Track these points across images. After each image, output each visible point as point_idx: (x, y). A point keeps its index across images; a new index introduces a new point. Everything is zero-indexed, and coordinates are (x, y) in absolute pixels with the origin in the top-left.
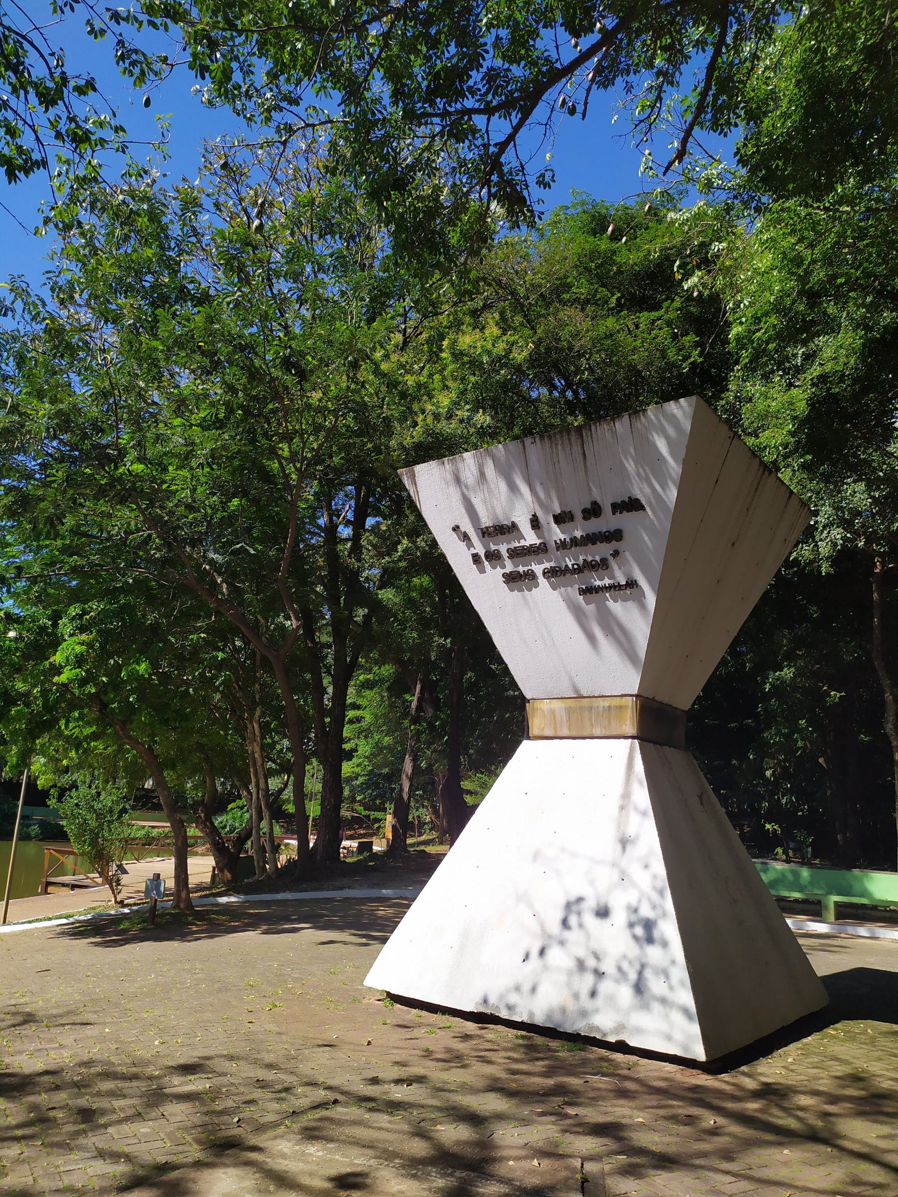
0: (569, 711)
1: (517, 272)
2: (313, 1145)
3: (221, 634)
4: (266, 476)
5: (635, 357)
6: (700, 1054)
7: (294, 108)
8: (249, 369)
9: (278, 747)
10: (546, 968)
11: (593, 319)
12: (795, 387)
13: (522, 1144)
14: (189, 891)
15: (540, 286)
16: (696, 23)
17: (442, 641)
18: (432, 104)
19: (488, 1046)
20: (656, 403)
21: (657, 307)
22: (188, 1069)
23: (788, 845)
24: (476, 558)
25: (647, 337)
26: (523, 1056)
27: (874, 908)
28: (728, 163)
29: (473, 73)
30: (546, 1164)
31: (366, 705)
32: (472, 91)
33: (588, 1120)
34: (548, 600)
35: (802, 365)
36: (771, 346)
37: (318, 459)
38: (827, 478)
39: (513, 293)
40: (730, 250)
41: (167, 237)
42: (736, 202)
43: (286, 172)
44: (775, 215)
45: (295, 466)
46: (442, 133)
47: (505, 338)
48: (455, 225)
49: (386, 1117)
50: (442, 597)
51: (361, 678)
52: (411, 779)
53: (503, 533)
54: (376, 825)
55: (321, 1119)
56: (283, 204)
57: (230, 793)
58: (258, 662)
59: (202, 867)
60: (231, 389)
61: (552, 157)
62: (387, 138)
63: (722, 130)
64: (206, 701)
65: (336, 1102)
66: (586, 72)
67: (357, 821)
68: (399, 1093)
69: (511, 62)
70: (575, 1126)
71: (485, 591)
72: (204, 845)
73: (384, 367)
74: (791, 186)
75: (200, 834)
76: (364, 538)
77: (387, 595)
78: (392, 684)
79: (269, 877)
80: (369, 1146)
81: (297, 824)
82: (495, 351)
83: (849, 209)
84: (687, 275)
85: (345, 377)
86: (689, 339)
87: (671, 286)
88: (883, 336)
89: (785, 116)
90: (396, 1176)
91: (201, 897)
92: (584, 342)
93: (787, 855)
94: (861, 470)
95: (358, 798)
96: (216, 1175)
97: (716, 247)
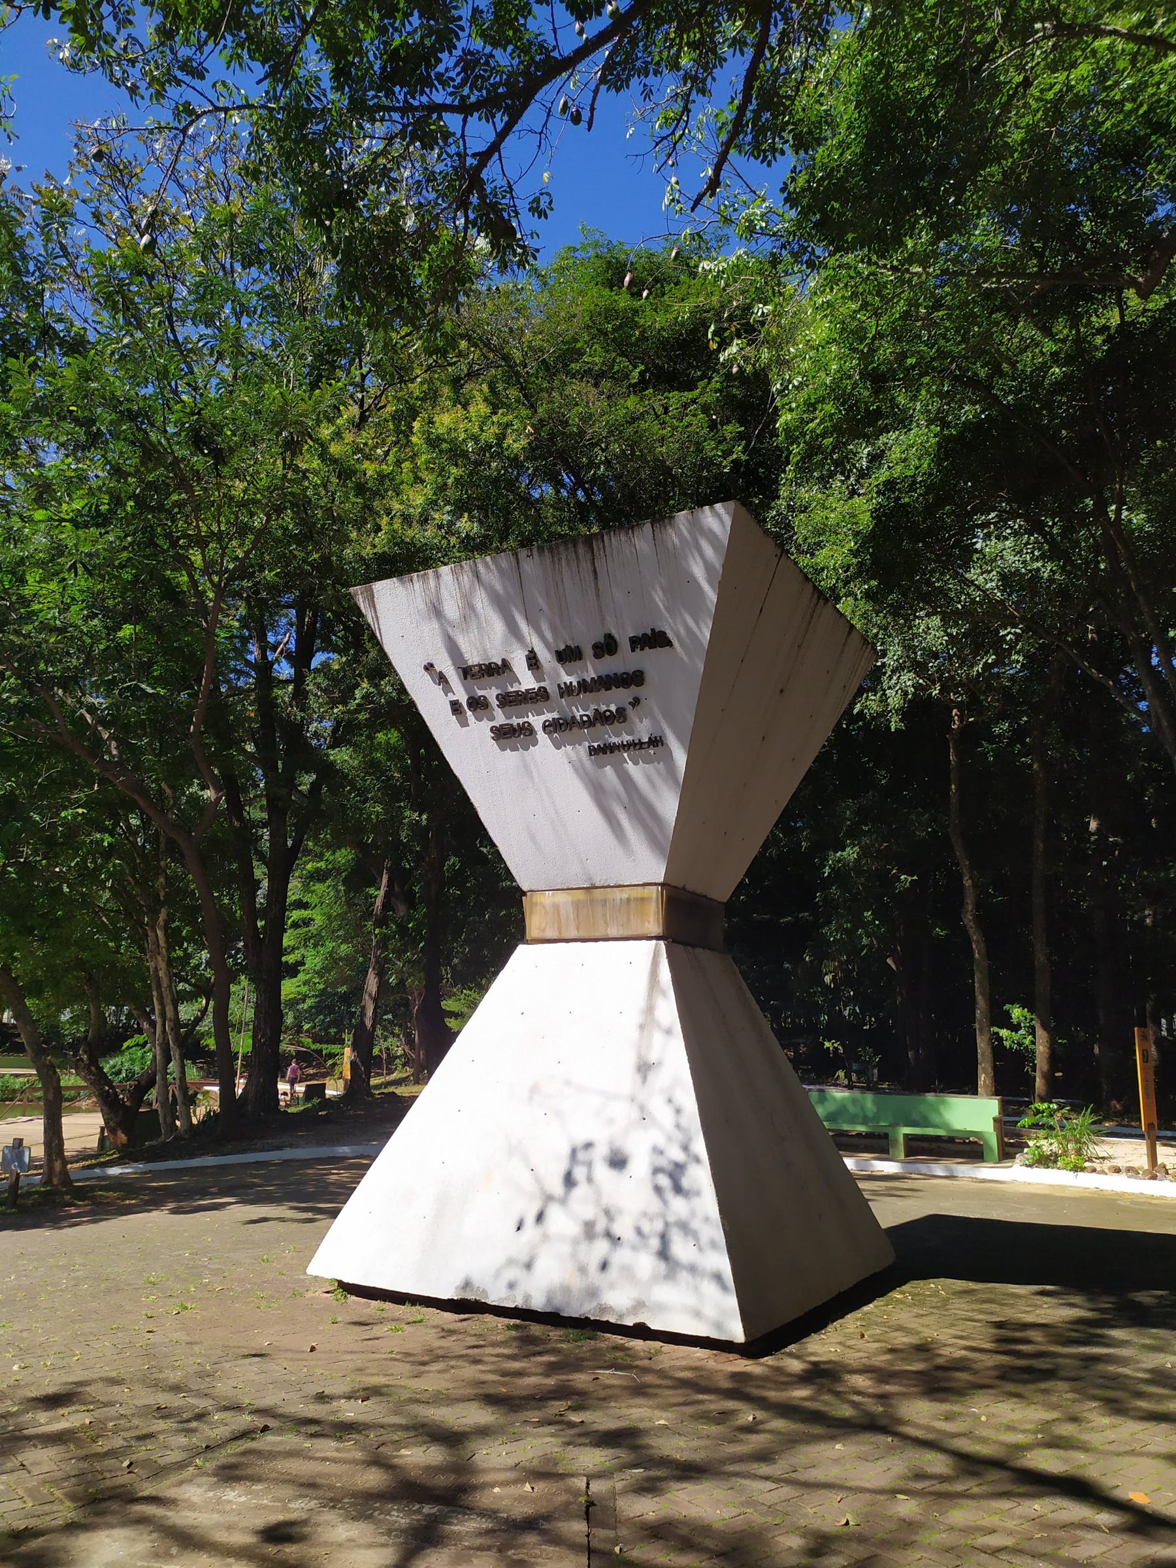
0: (577, 905)
1: (511, 330)
2: (233, 1489)
3: (108, 809)
4: (171, 593)
5: (664, 449)
6: (737, 1332)
7: (196, 83)
8: (142, 446)
9: (193, 962)
10: (546, 1238)
11: (609, 397)
12: (859, 495)
13: (506, 1463)
14: (65, 1162)
15: (542, 350)
16: (732, 17)
17: (415, 816)
18: (390, 93)
19: (472, 1341)
20: (690, 508)
21: (690, 386)
22: (53, 1401)
23: (851, 1066)
24: (456, 707)
25: (676, 424)
26: (516, 1351)
27: (951, 1140)
28: (775, 201)
29: (444, 56)
30: (541, 1486)
31: (314, 902)
32: (443, 80)
33: (596, 1427)
34: (554, 764)
35: (868, 468)
36: (828, 441)
37: (243, 570)
38: (895, 611)
39: (506, 358)
40: (778, 314)
41: (24, 257)
42: (784, 253)
43: (192, 172)
44: (831, 272)
45: (211, 581)
46: (402, 134)
47: (495, 419)
48: (422, 259)
49: (333, 1444)
50: (415, 757)
51: (309, 866)
52: (376, 1000)
53: (490, 674)
54: (330, 1062)
55: (245, 1453)
56: (189, 221)
57: (127, 1027)
58: (162, 846)
59: (83, 1128)
60: (117, 472)
61: (551, 178)
62: (327, 137)
63: (765, 157)
64: (87, 902)
65: (265, 1429)
66: (592, 67)
67: (305, 1058)
68: (351, 1411)
69: (495, 44)
70: (580, 1435)
71: (468, 750)
72: (89, 1097)
73: (335, 449)
74: (850, 237)
75: (84, 1084)
76: (309, 679)
77: (341, 756)
78: (350, 874)
79: (178, 1138)
80: (309, 1485)
81: (220, 1065)
82: (484, 436)
83: (920, 270)
84: (724, 344)
85: (279, 463)
86: (731, 429)
87: (708, 360)
88: (961, 433)
89: (843, 146)
90: (345, 1521)
91: (84, 1168)
92: (598, 428)
93: (850, 1080)
94: (935, 600)
95: (306, 1027)
96: (96, 1540)
97: (760, 309)
